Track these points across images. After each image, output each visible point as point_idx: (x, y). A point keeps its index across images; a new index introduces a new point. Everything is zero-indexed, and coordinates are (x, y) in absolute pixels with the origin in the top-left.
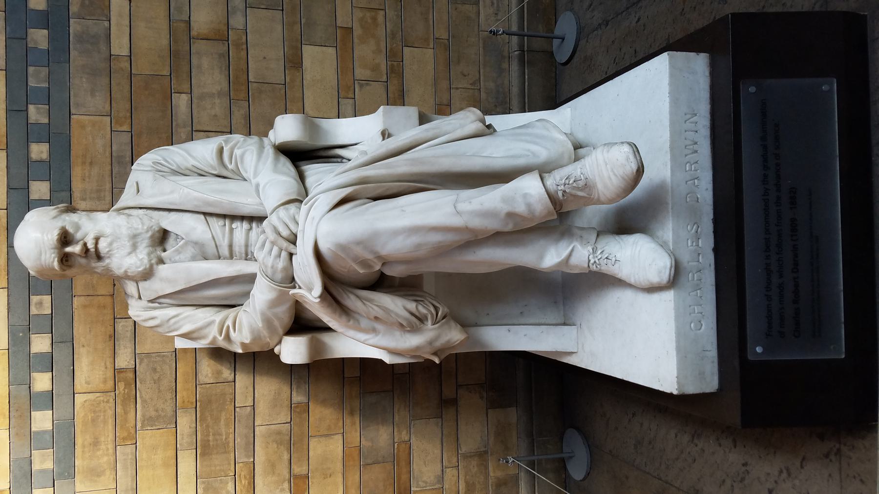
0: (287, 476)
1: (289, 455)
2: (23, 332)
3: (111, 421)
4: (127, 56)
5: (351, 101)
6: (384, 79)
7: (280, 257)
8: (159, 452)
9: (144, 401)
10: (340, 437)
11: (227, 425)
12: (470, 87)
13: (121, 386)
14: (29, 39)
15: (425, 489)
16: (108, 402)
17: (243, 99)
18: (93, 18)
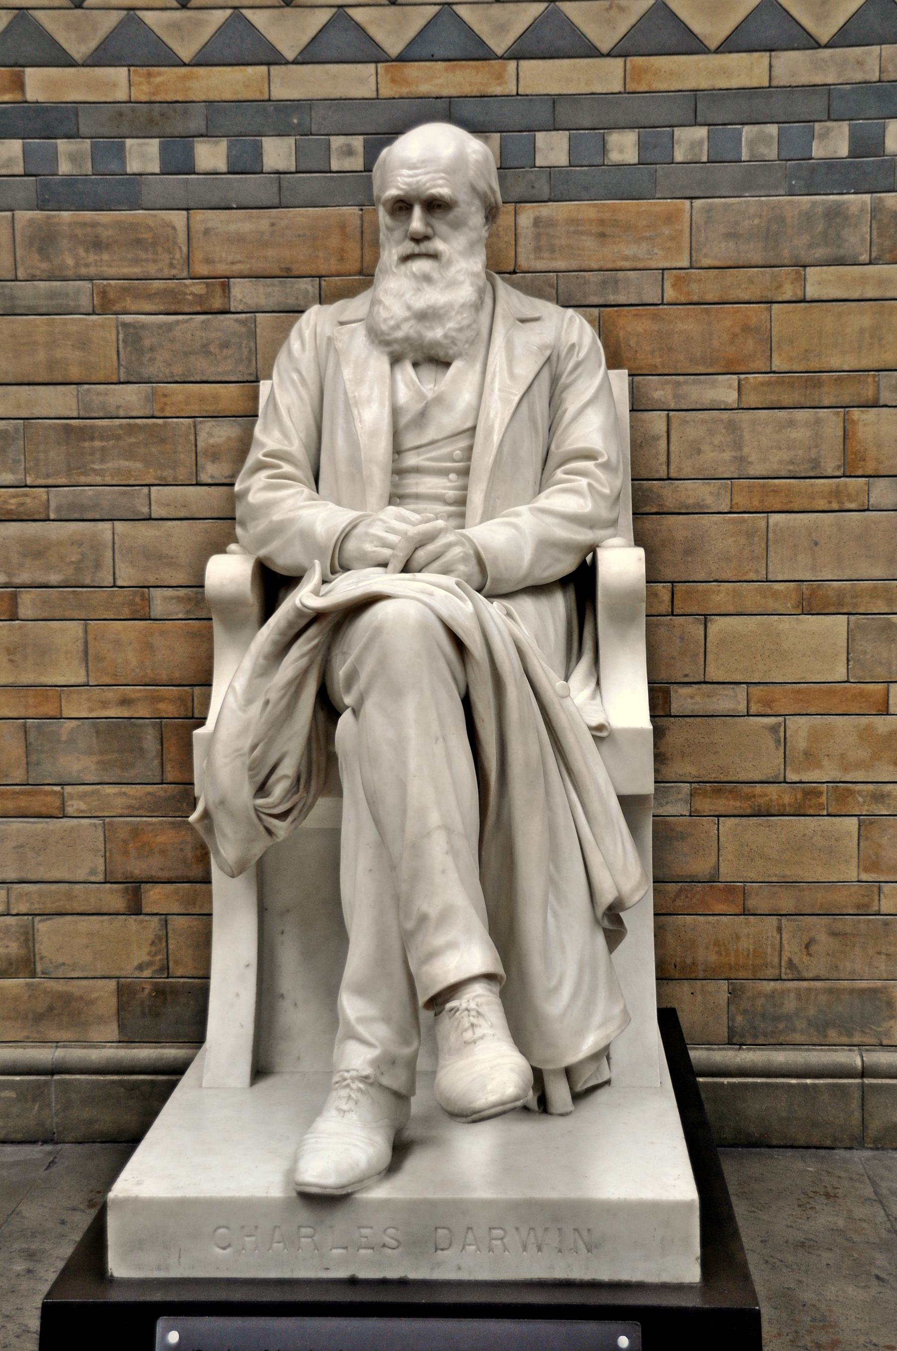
0: (17, 580)
1: (56, 584)
2: (299, 124)
3: (136, 270)
5: (742, 708)
6: (792, 777)
7: (383, 547)
8: (77, 353)
9: (169, 327)
10: (82, 680)
11: (118, 472)
12: (785, 958)
13: (198, 288)
14: (829, 124)
16: (172, 266)
17: (734, 502)
18: (875, 233)
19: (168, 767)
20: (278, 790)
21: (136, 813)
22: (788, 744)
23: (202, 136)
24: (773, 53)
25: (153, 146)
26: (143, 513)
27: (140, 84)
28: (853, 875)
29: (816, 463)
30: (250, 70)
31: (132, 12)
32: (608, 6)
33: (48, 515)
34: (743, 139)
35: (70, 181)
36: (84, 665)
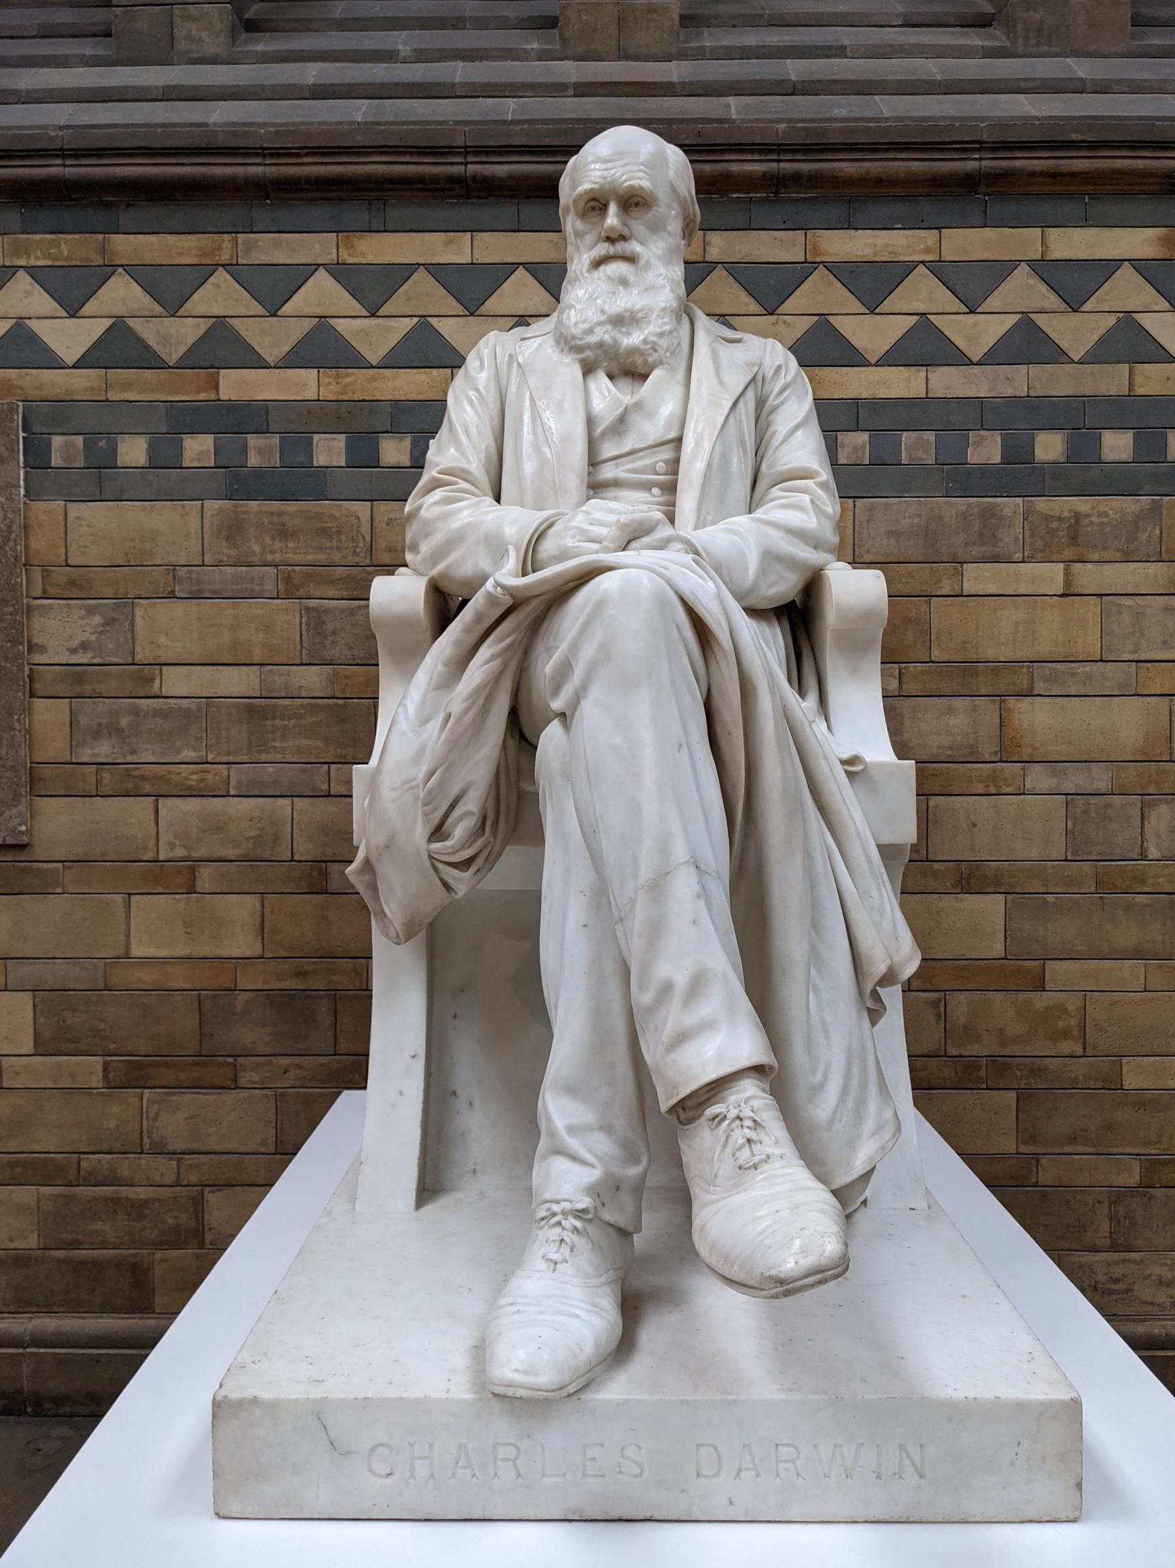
0: (195, 855)
1: (234, 858)
3: (321, 558)
4: (962, 590)
6: (953, 1051)
8: (261, 635)
10: (258, 951)
14: (983, 433)
15: (145, 1115)
16: (355, 554)
19: (341, 1039)
21: (308, 1084)
22: (948, 1020)
23: (387, 432)
24: (929, 368)
25: (340, 441)
26: (322, 790)
27: (329, 384)
28: (1013, 1149)
29: (973, 749)
30: (434, 371)
31: (323, 320)
32: (775, 322)
33: (229, 791)
35: (259, 473)
36: (260, 937)
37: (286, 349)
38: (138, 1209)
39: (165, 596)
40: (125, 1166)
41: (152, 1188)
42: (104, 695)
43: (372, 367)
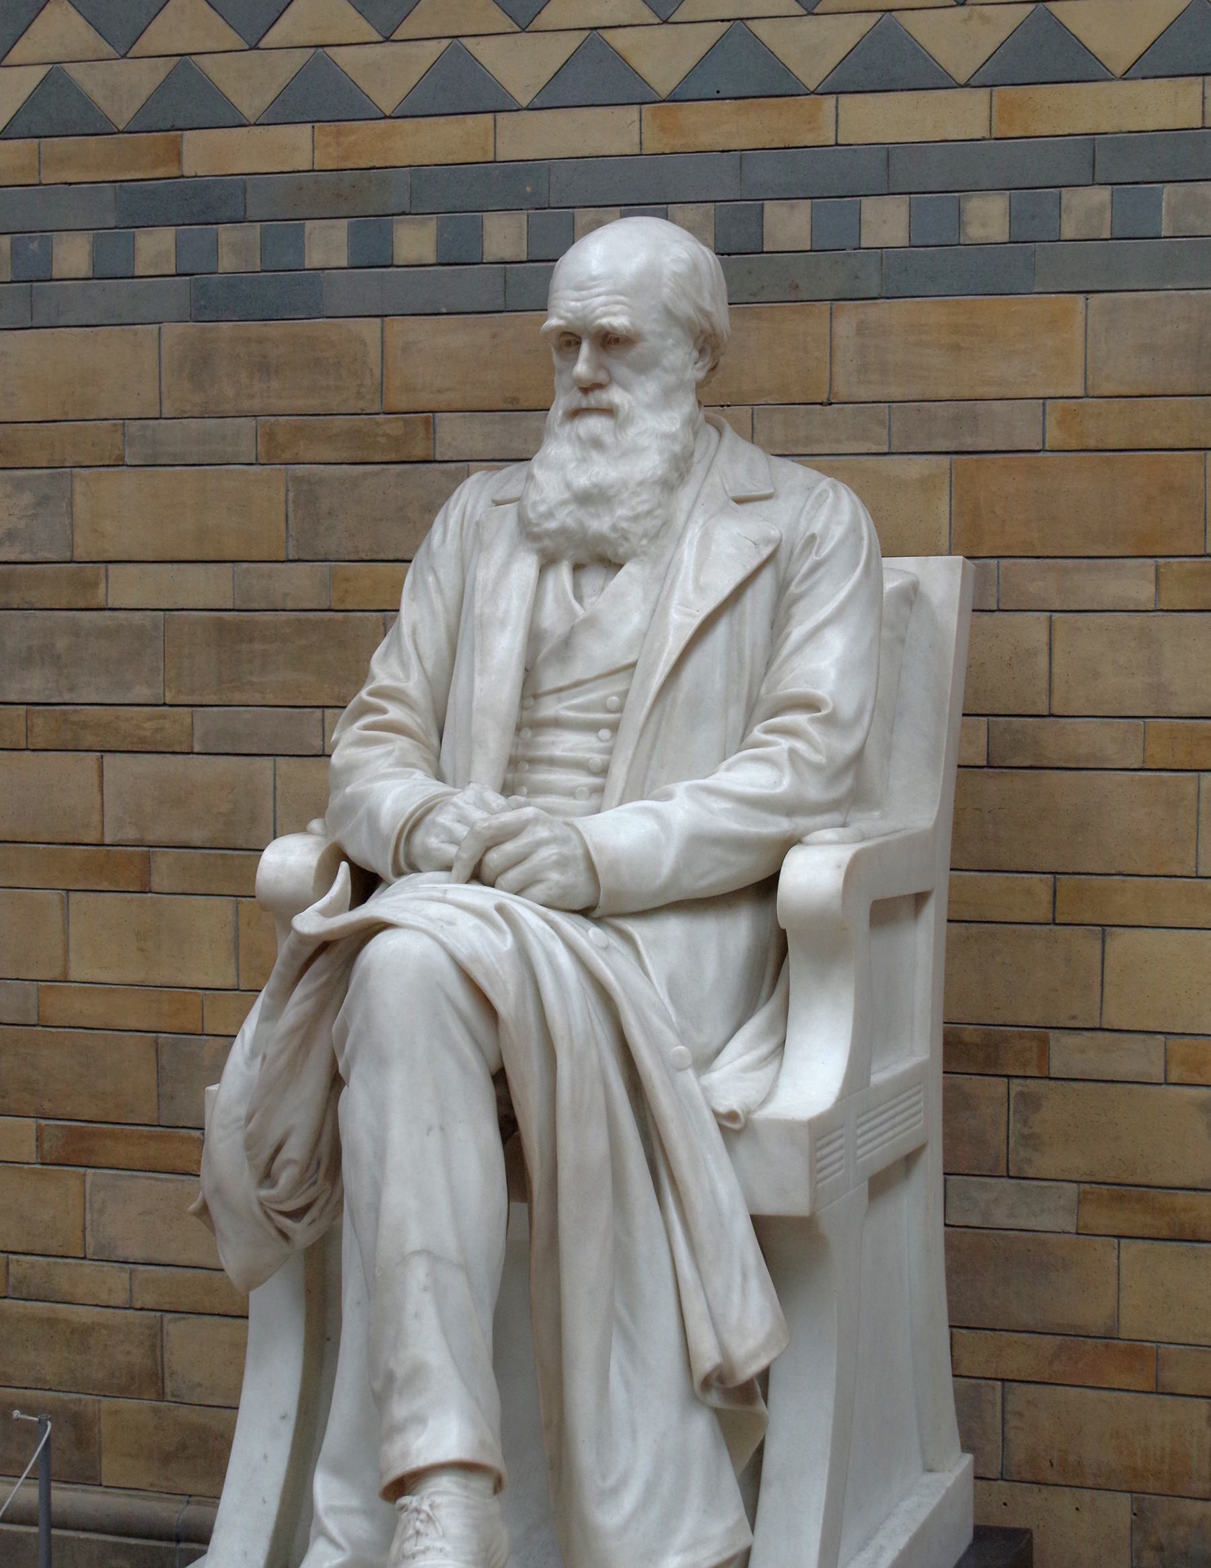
0: (150, 838)
1: (199, 844)
3: (314, 403)
10: (230, 982)
15: (88, 1205)
20: (286, 1178)
23: (403, 214)
25: (339, 231)
31: (320, 50)
34: (1164, 204)
37: (269, 98)
38: (81, 1335)
39: (112, 463)
40: (63, 1275)
41: (98, 1309)
42: (36, 606)
43: (386, 117)
